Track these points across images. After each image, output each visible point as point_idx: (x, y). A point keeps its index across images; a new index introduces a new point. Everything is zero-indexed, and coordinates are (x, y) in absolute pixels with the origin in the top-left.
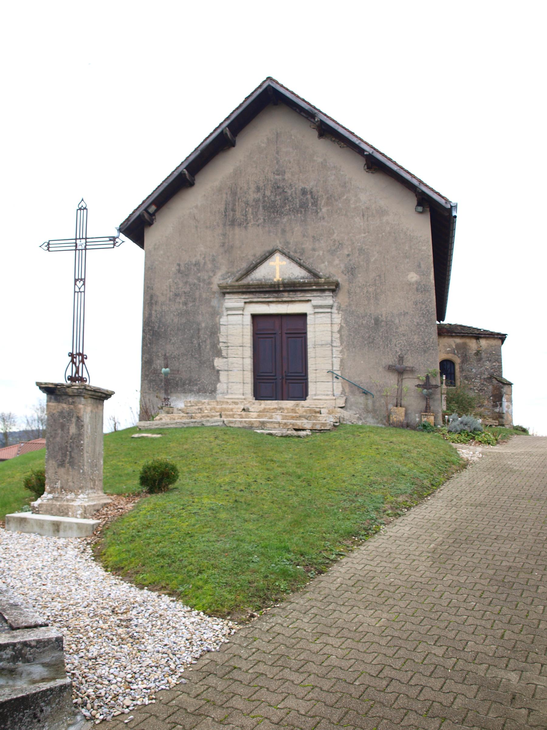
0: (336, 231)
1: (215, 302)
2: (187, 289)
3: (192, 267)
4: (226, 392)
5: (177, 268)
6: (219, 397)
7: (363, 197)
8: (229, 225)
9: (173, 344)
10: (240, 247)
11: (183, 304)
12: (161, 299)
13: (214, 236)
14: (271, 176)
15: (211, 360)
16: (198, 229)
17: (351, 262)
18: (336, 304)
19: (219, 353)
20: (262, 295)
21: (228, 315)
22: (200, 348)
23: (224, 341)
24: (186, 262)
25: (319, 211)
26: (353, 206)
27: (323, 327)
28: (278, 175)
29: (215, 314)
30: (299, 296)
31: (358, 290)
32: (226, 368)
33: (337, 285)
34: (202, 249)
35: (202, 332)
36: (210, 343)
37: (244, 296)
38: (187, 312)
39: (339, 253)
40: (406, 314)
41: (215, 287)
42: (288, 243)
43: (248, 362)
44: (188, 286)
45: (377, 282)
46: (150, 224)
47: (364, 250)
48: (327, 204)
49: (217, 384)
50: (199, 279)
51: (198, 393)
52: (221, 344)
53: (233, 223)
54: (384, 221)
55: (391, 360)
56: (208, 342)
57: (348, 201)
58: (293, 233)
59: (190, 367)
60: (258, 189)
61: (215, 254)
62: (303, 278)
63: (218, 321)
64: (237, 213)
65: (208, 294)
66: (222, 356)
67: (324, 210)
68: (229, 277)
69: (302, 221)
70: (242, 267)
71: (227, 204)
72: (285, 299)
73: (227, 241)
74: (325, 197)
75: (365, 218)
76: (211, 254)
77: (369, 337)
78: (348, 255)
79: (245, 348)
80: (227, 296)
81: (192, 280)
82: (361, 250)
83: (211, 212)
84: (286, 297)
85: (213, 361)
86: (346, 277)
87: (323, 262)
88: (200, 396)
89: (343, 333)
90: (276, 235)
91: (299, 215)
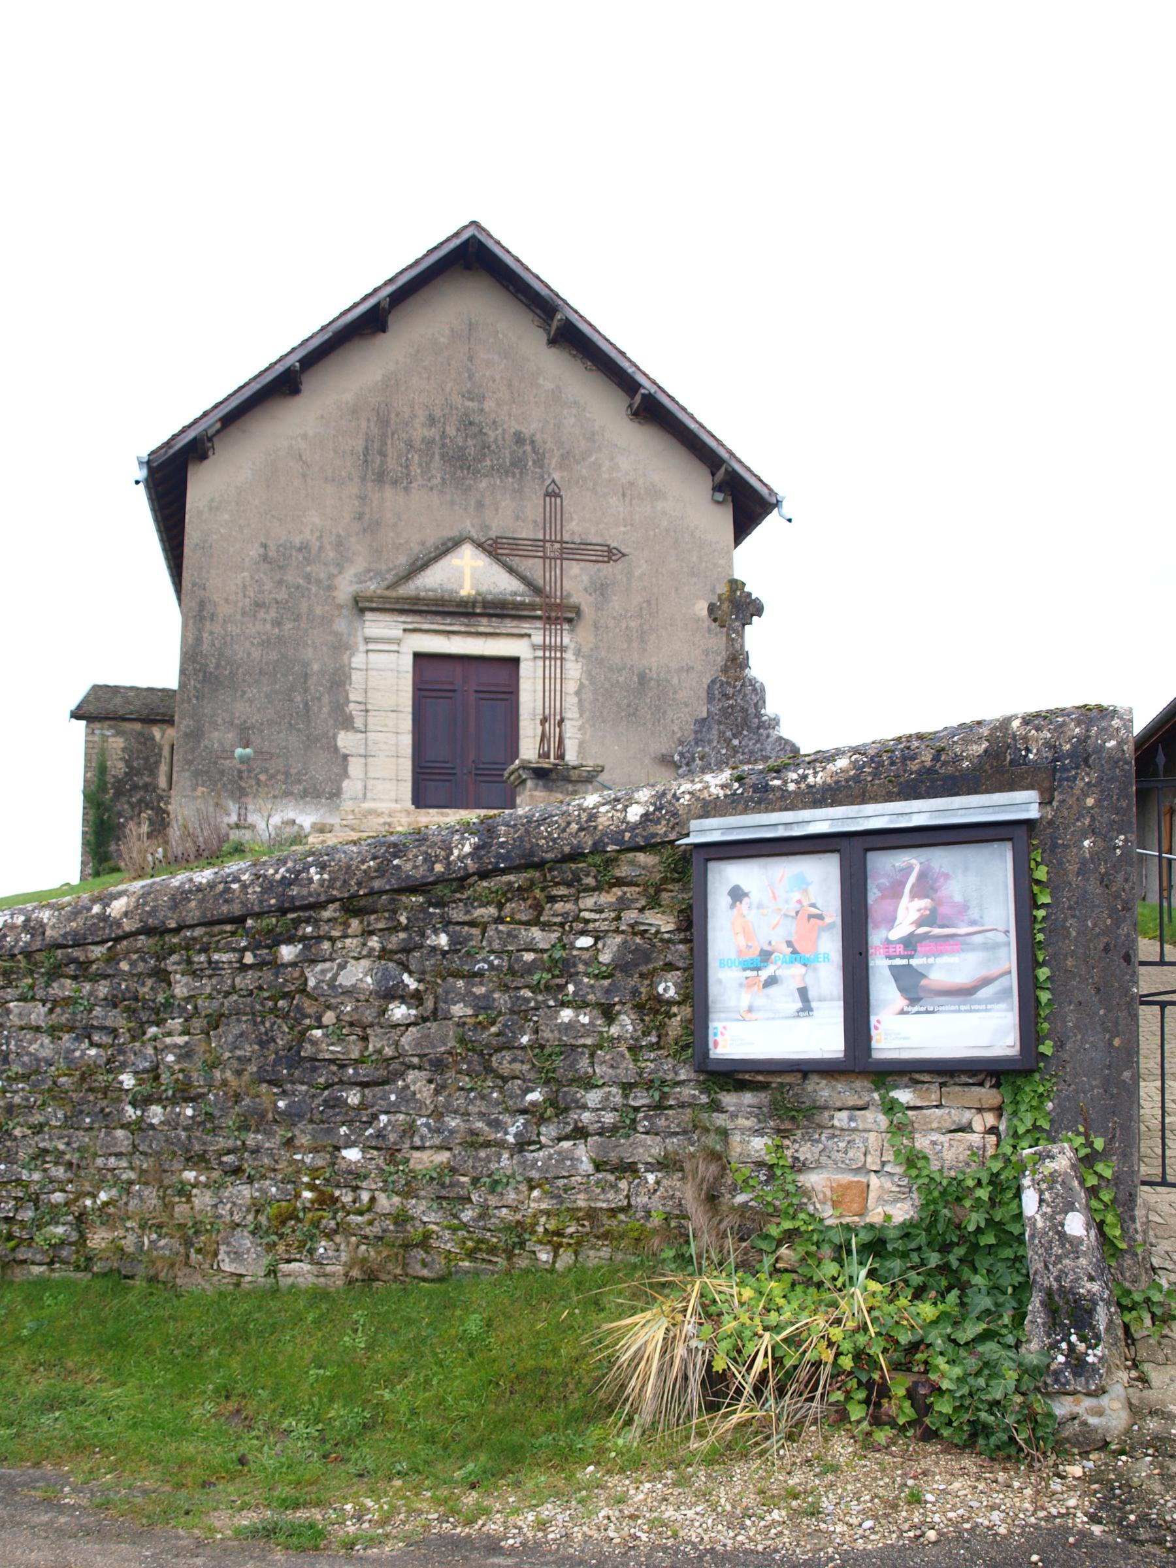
0: (575, 516)
1: (341, 625)
2: (282, 595)
3: (294, 553)
4: (361, 796)
5: (262, 551)
6: (347, 805)
7: (624, 463)
8: (373, 481)
9: (251, 701)
10: (395, 525)
11: (273, 625)
12: (224, 610)
13: (340, 498)
14: (457, 400)
15: (331, 734)
16: (309, 480)
19: (347, 723)
20: (439, 619)
21: (367, 651)
22: (308, 711)
23: (359, 699)
24: (281, 542)
26: (606, 476)
28: (472, 400)
29: (341, 647)
30: (509, 626)
31: (611, 624)
32: (362, 752)
33: (577, 610)
34: (316, 520)
35: (312, 682)
36: (330, 702)
37: (403, 618)
38: (281, 640)
43: (406, 741)
44: (284, 589)
45: (644, 612)
46: (203, 457)
49: (342, 781)
50: (308, 578)
51: (302, 798)
52: (352, 706)
53: (381, 477)
54: (659, 508)
56: (326, 699)
57: (597, 466)
58: (497, 510)
59: (285, 748)
60: (432, 421)
61: (342, 534)
62: (515, 594)
63: (346, 661)
64: (389, 459)
65: (327, 608)
66: (353, 728)
68: (371, 579)
69: (514, 491)
70: (398, 563)
71: (368, 439)
72: (481, 629)
73: (367, 510)
74: (557, 453)
75: (627, 499)
76: (334, 531)
77: (629, 706)
79: (401, 715)
80: (369, 616)
81: (291, 577)
83: (335, 451)
84: (484, 625)
85: (335, 737)
86: (591, 599)
88: (307, 803)
89: (584, 696)
90: (465, 509)
91: (510, 479)
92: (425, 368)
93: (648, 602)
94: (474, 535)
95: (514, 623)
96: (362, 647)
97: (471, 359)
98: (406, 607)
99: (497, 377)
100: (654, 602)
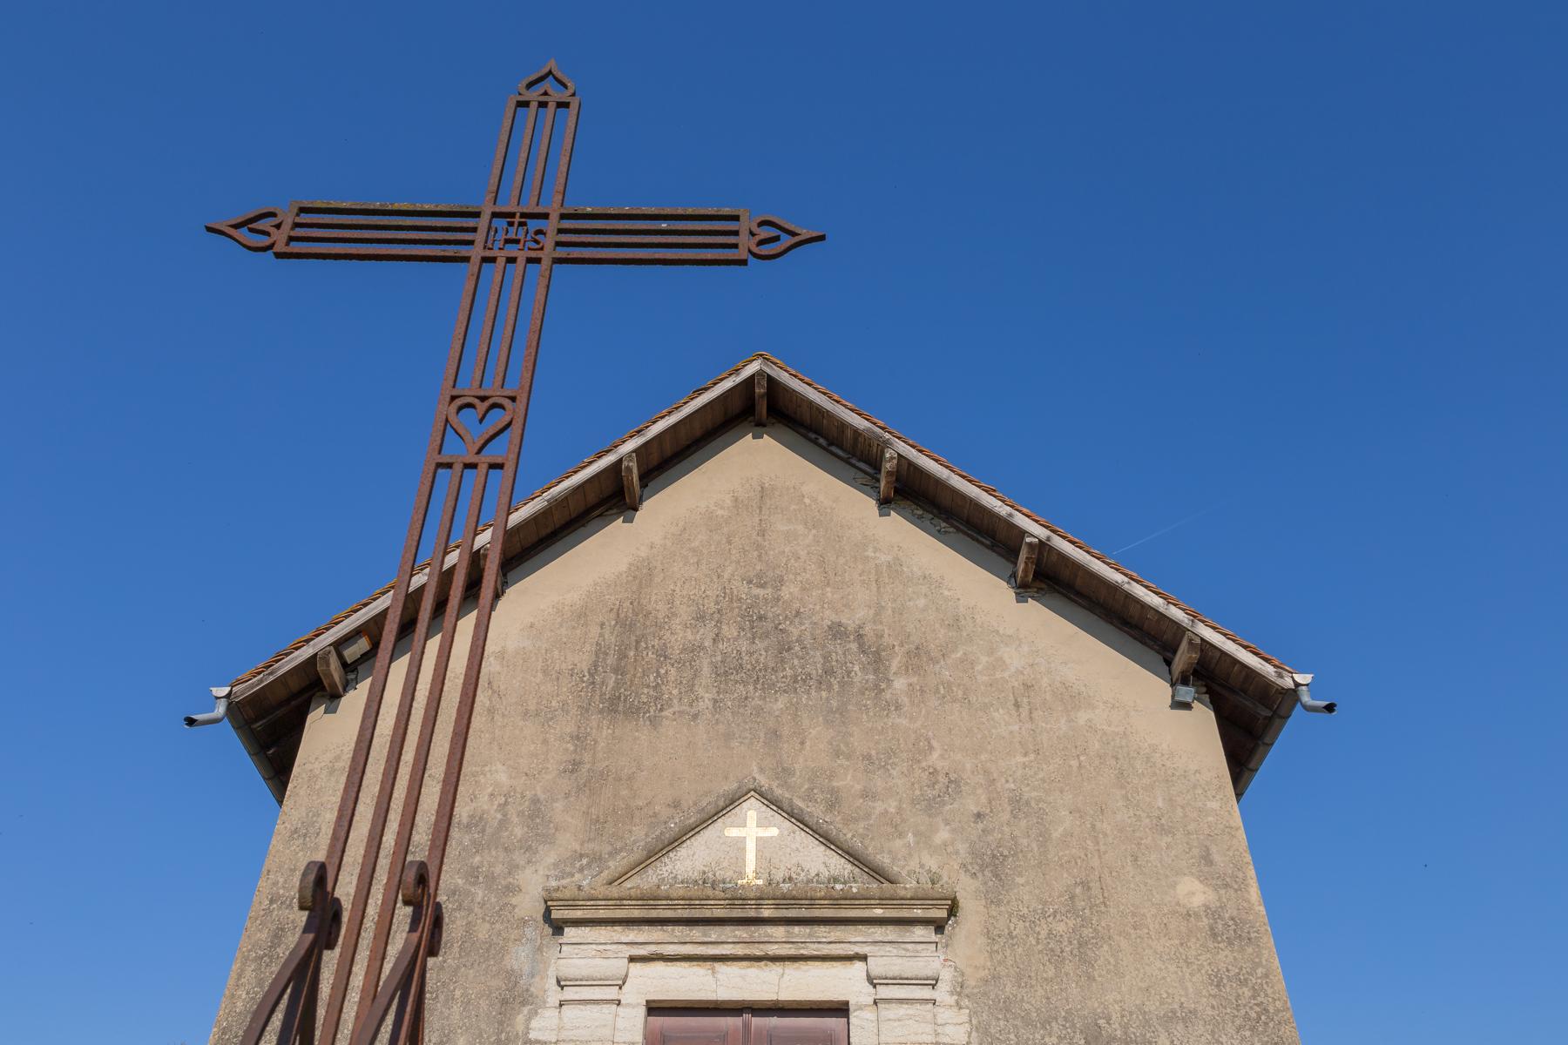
0: (935, 743)
1: (519, 957)
7: (1014, 659)
8: (601, 712)
13: (545, 741)
14: (741, 589)
17: (990, 838)
18: (946, 975)
20: (696, 933)
25: (883, 686)
28: (762, 586)
34: (502, 777)
37: (633, 934)
39: (948, 807)
40: (1189, 1017)
41: (529, 904)
42: (788, 772)
45: (1080, 904)
47: (1028, 803)
48: (907, 669)
54: (1081, 722)
58: (802, 743)
60: (701, 617)
61: (542, 797)
63: (520, 1028)
67: (900, 684)
71: (601, 652)
72: (773, 950)
73: (587, 757)
75: (1024, 712)
78: (979, 816)
80: (570, 933)
82: (1018, 804)
83: (545, 672)
87: (901, 835)
92: (694, 550)
93: (1085, 885)
94: (763, 781)
97: (762, 533)
98: (636, 914)
99: (803, 554)
100: (1095, 886)
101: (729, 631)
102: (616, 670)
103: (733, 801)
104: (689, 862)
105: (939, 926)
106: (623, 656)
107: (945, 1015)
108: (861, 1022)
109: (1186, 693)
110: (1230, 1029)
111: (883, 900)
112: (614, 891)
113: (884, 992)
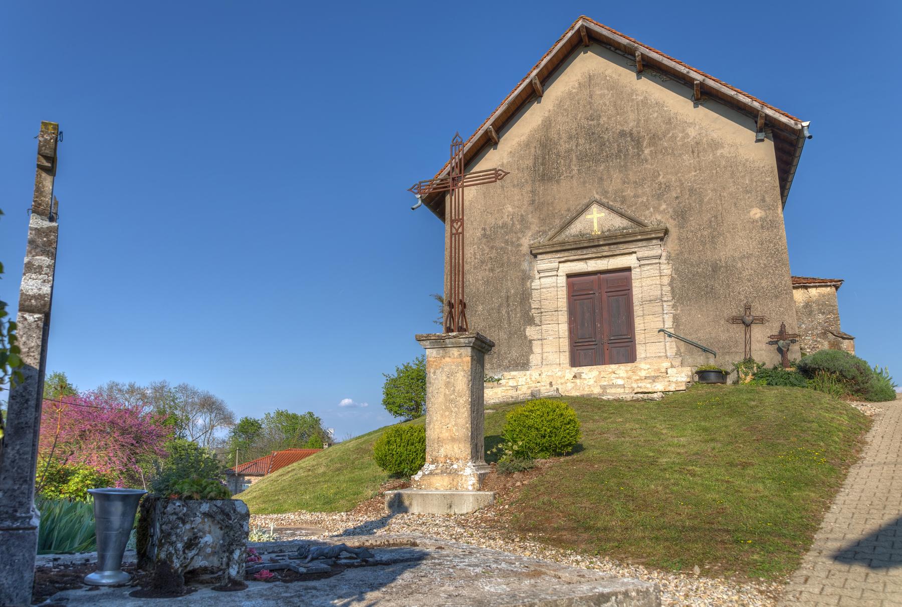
1: (525, 266)
7: (692, 132)
20: (579, 252)
26: (679, 143)
27: (650, 276)
28: (593, 120)
29: (526, 277)
32: (540, 337)
34: (510, 209)
37: (559, 255)
41: (525, 249)
42: (607, 192)
48: (649, 145)
50: (506, 242)
55: (735, 311)
57: (674, 137)
60: (570, 138)
62: (624, 228)
67: (647, 151)
71: (536, 158)
73: (537, 198)
75: (696, 154)
78: (677, 198)
80: (539, 257)
81: (499, 244)
82: (692, 191)
92: (565, 110)
94: (597, 197)
95: (625, 246)
96: (537, 276)
97: (591, 97)
98: (559, 248)
99: (607, 103)
100: (719, 218)
101: (582, 141)
102: (543, 164)
103: (587, 207)
104: (576, 228)
105: (661, 239)
106: (544, 158)
107: (663, 267)
108: (635, 273)
109: (761, 136)
110: (764, 258)
111: (641, 233)
112: (551, 243)
113: (643, 262)
